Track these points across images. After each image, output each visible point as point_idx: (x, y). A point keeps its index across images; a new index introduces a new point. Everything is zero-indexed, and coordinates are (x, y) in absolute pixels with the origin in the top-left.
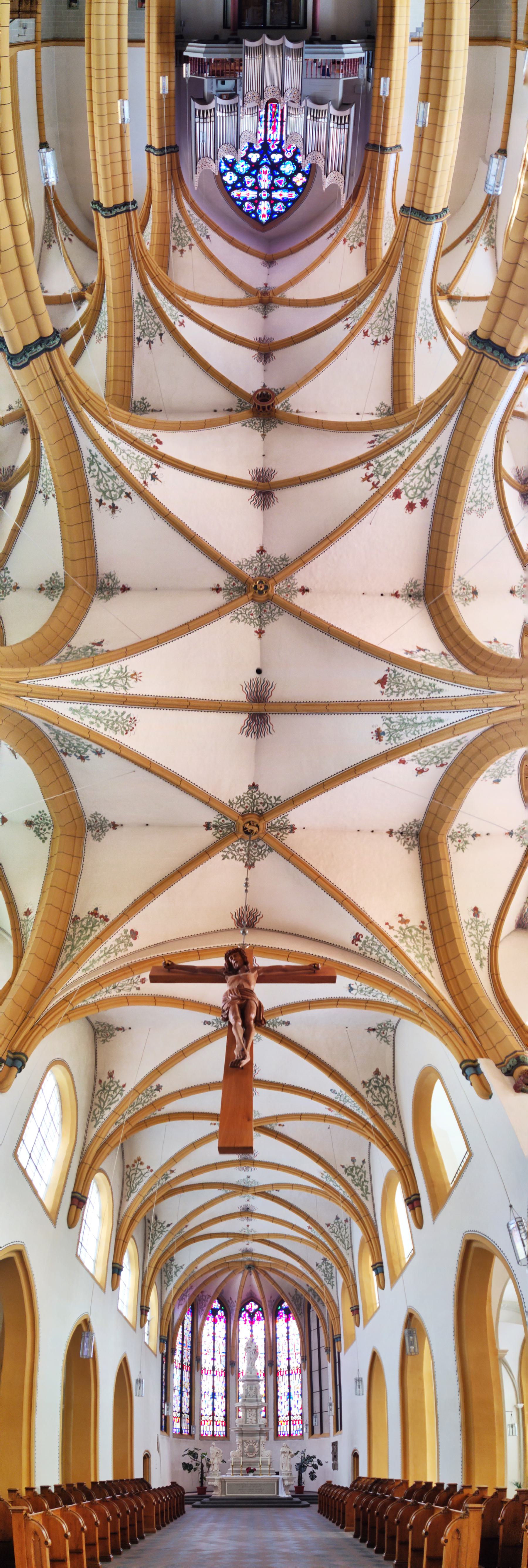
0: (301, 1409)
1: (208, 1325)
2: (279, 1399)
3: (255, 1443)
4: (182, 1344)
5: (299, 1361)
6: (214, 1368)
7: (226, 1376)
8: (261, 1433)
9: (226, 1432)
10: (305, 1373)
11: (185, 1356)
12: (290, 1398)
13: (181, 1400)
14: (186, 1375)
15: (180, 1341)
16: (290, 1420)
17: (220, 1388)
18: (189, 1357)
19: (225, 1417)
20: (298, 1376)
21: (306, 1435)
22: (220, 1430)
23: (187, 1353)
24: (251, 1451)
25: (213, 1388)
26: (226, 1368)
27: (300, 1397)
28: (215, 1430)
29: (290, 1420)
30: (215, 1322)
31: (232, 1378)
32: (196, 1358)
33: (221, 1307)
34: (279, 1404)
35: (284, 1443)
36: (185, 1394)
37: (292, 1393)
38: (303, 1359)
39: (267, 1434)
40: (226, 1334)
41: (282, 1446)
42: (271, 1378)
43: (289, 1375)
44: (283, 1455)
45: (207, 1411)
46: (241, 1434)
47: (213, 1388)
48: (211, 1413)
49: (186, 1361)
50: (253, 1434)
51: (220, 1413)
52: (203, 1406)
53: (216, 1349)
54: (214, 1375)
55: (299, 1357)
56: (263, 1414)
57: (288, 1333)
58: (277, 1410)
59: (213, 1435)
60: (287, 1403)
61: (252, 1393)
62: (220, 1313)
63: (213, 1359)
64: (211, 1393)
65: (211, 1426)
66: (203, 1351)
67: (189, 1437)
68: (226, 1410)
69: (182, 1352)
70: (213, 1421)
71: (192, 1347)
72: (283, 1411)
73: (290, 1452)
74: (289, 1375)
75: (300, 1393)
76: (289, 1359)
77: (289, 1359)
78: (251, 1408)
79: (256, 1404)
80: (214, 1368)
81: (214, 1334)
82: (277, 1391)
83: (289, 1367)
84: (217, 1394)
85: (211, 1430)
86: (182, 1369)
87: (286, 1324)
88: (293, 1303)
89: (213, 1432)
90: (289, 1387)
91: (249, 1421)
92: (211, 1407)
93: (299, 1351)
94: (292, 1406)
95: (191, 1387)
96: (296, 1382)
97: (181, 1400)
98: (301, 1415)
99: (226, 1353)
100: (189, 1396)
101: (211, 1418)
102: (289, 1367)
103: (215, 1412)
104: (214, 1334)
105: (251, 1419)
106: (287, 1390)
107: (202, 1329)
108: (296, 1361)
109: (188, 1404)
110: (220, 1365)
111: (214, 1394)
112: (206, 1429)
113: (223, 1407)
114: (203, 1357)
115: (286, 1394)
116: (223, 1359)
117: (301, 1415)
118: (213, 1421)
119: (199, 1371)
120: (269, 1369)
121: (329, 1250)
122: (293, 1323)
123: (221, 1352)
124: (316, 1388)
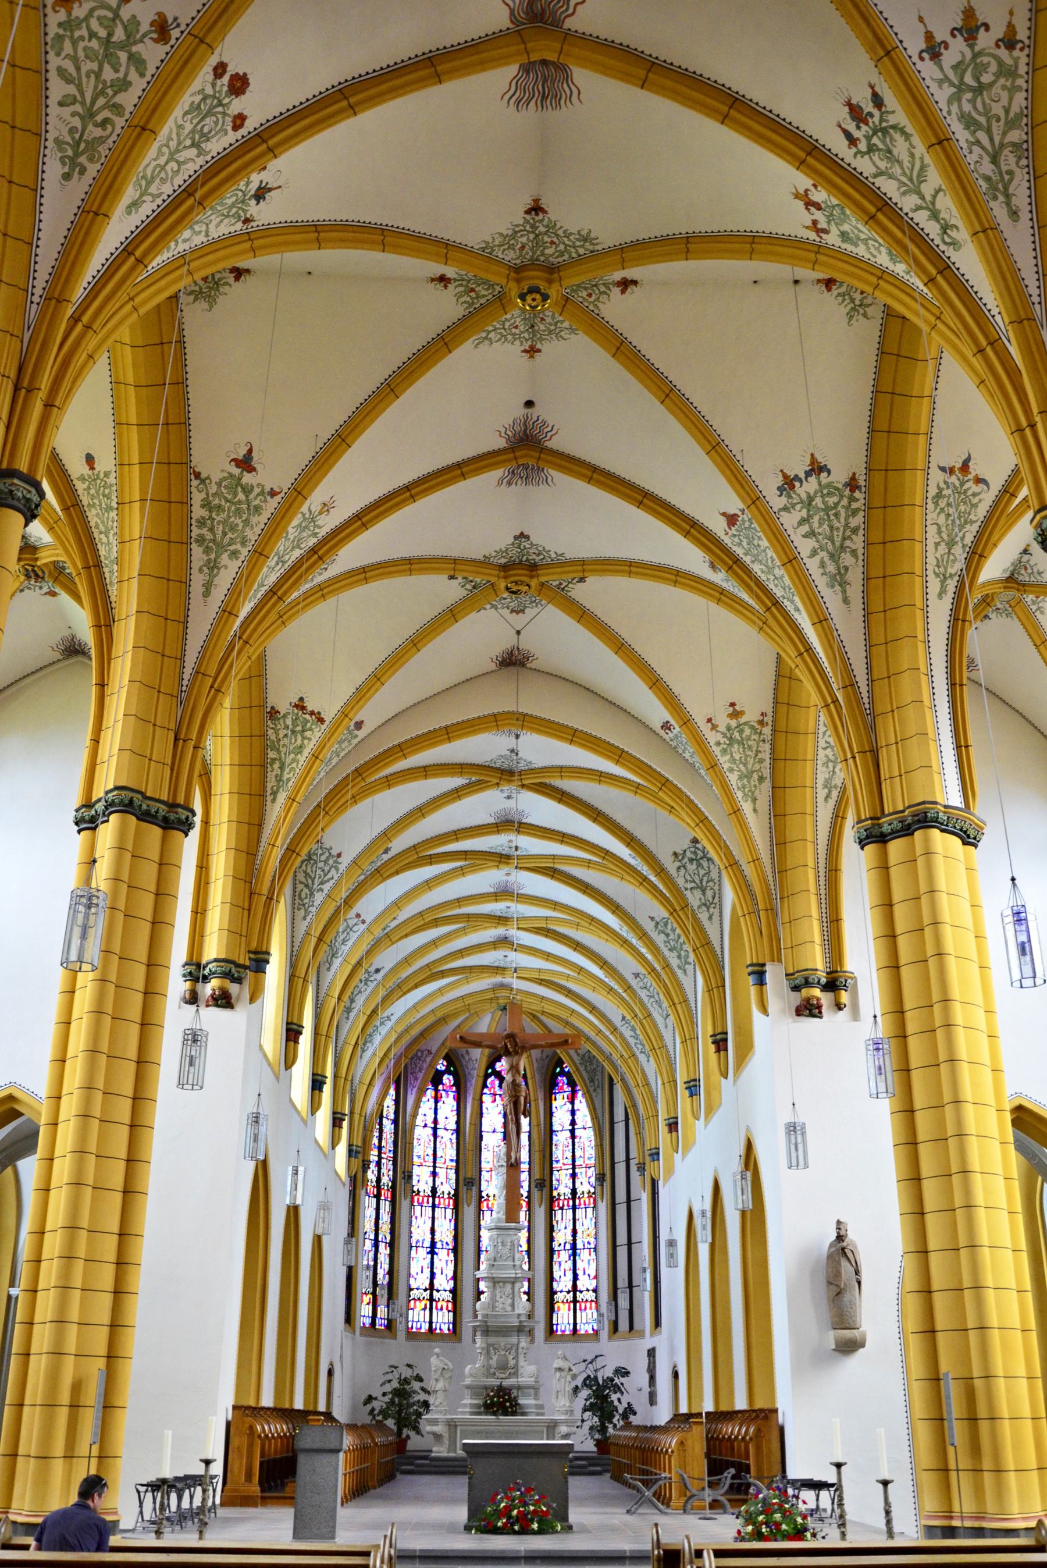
0: (596, 1277)
1: (426, 1106)
2: (555, 1257)
3: (508, 1350)
4: (380, 1148)
5: (593, 1180)
6: (434, 1190)
7: (456, 1208)
8: (520, 1329)
9: (454, 1323)
10: (603, 1207)
11: (384, 1170)
12: (574, 1254)
13: (376, 1259)
14: (385, 1207)
15: (375, 1141)
16: (575, 1301)
17: (445, 1231)
18: (391, 1173)
19: (454, 1291)
20: (590, 1211)
21: (604, 1334)
22: (443, 1320)
23: (387, 1166)
24: (503, 1367)
25: (433, 1231)
26: (456, 1190)
27: (593, 1254)
28: (434, 1320)
29: (575, 1301)
30: (437, 1099)
31: (468, 1212)
32: (403, 1174)
33: (448, 1067)
34: (556, 1267)
35: (561, 1349)
36: (382, 1246)
37: (579, 1245)
38: (600, 1178)
39: (531, 1333)
40: (458, 1123)
41: (558, 1356)
42: (540, 1213)
43: (574, 1208)
44: (558, 1374)
45: (420, 1281)
46: (487, 1331)
47: (433, 1231)
48: (427, 1284)
49: (385, 1180)
50: (503, 1331)
51: (444, 1283)
52: (415, 1268)
53: (439, 1153)
54: (434, 1207)
55: (591, 1172)
56: (526, 1288)
57: (573, 1123)
58: (551, 1279)
59: (431, 1329)
60: (570, 1264)
61: (505, 1251)
62: (448, 1080)
63: (434, 1174)
64: (427, 1244)
65: (427, 1311)
66: (416, 1160)
67: (387, 1333)
68: (455, 1278)
69: (379, 1164)
70: (431, 1299)
71: (395, 1152)
72: (563, 1283)
73: (570, 1370)
74: (574, 1208)
75: (592, 1246)
76: (574, 1176)
77: (574, 1176)
78: (505, 1281)
79: (511, 1274)
80: (434, 1190)
81: (435, 1121)
82: (552, 1239)
83: (574, 1191)
84: (439, 1245)
85: (427, 1319)
86: (378, 1197)
87: (569, 1106)
88: (582, 1069)
89: (431, 1323)
90: (574, 1232)
91: (499, 1305)
92: (427, 1272)
93: (593, 1161)
94: (580, 1272)
95: (392, 1231)
96: (586, 1222)
97: (376, 1259)
98: (595, 1291)
99: (457, 1161)
100: (388, 1251)
101: (427, 1295)
102: (574, 1191)
103: (435, 1282)
104: (435, 1121)
105: (503, 1303)
106: (570, 1238)
107: (415, 1115)
108: (586, 1183)
109: (386, 1267)
110: (446, 1185)
111: (433, 1244)
112: (418, 1317)
113: (450, 1271)
114: (416, 1170)
115: (568, 1247)
116: (452, 1175)
117: (595, 1291)
118: (431, 1299)
119: (408, 1200)
120: (536, 1193)
121: (654, 970)
122: (581, 1104)
123: (448, 1158)
124: (622, 1238)
